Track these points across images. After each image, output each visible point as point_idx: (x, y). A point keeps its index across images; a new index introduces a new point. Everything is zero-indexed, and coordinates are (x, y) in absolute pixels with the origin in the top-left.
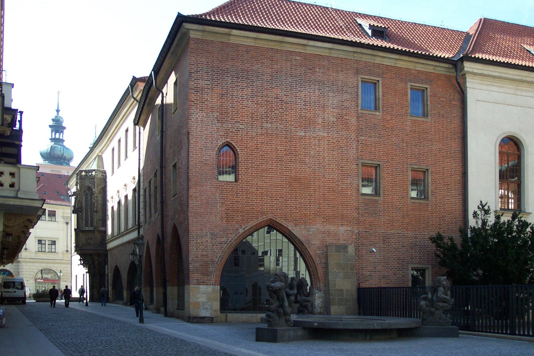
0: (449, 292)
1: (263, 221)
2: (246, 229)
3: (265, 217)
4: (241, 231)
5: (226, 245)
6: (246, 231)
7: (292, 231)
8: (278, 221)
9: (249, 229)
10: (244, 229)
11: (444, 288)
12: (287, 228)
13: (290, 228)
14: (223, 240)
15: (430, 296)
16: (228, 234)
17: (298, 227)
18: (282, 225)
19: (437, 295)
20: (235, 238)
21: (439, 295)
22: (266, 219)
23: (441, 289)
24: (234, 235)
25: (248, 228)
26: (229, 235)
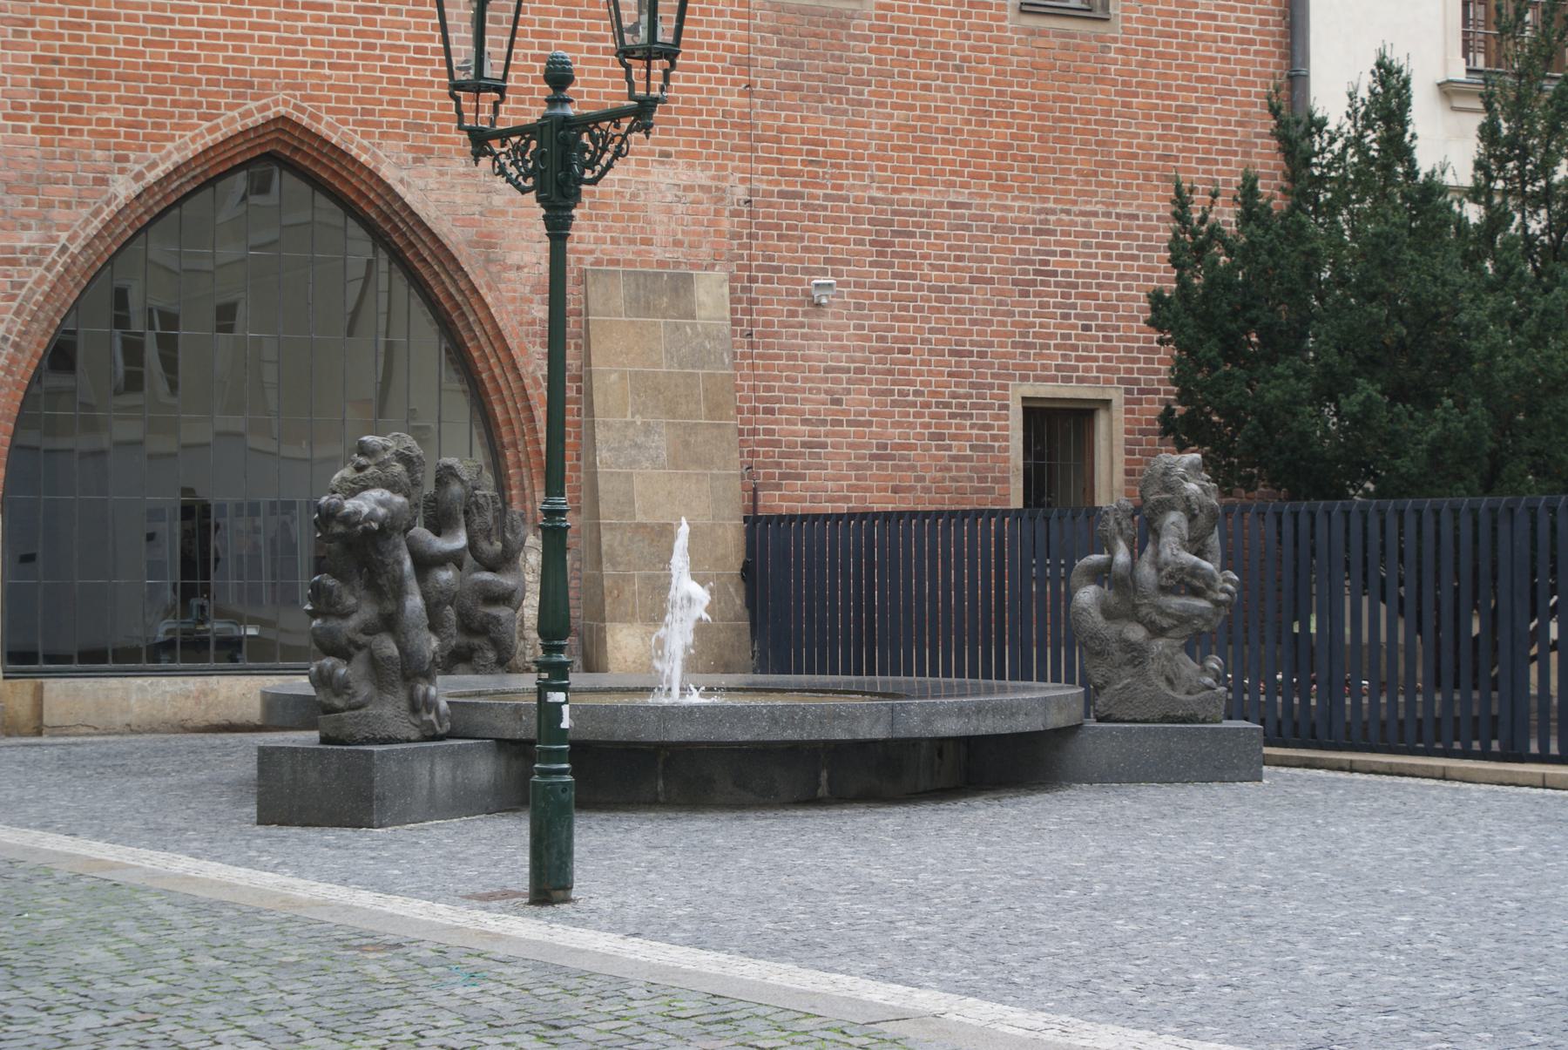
0: (1214, 540)
1: (244, 133)
2: (151, 177)
3: (251, 105)
4: (123, 188)
5: (38, 271)
6: (147, 190)
7: (399, 189)
8: (323, 129)
9: (168, 176)
10: (139, 177)
11: (1192, 518)
12: (372, 173)
13: (388, 173)
14: (26, 239)
15: (1122, 556)
16: (49, 205)
17: (431, 167)
18: (344, 154)
19: (1157, 554)
20: (92, 230)
21: (1166, 553)
22: (258, 118)
23: (1175, 518)
24: (85, 212)
25: (159, 172)
26: (58, 214)
